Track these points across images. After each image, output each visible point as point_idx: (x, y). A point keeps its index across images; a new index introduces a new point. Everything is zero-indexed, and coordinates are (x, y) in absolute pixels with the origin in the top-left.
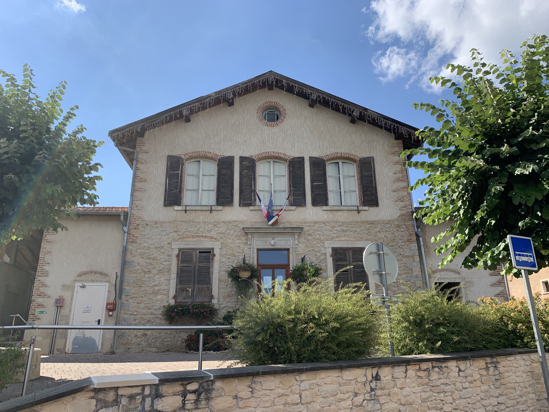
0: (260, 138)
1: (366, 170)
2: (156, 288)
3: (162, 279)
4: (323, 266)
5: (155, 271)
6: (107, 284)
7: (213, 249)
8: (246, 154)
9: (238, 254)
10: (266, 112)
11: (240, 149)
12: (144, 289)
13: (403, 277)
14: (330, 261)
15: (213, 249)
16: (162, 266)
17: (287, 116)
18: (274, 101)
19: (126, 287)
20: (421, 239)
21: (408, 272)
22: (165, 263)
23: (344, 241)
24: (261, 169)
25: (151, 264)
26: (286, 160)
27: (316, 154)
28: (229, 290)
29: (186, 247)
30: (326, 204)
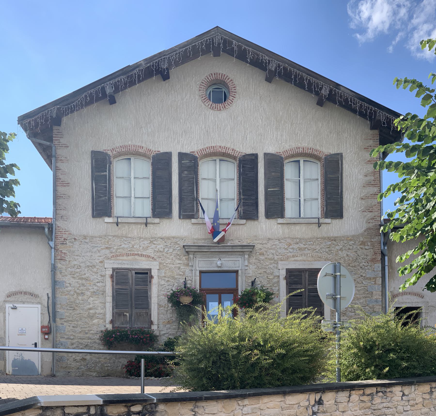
0: (203, 127)
1: (332, 169)
2: (91, 311)
3: (96, 302)
4: (275, 290)
5: (89, 293)
6: (39, 306)
7: (150, 270)
8: (187, 150)
9: (178, 277)
10: (211, 89)
11: (178, 142)
12: (78, 312)
13: (361, 301)
14: (283, 284)
15: (150, 270)
16: (96, 288)
17: (237, 96)
18: (221, 72)
19: (59, 310)
20: (386, 258)
21: (368, 295)
22: (98, 284)
23: (301, 261)
24: (206, 170)
25: (83, 285)
26: (234, 158)
27: (272, 149)
28: (169, 316)
29: (120, 266)
30: (282, 216)
